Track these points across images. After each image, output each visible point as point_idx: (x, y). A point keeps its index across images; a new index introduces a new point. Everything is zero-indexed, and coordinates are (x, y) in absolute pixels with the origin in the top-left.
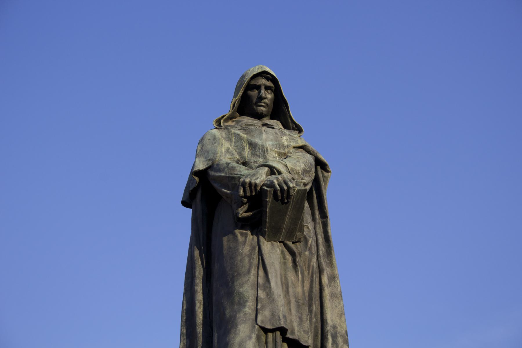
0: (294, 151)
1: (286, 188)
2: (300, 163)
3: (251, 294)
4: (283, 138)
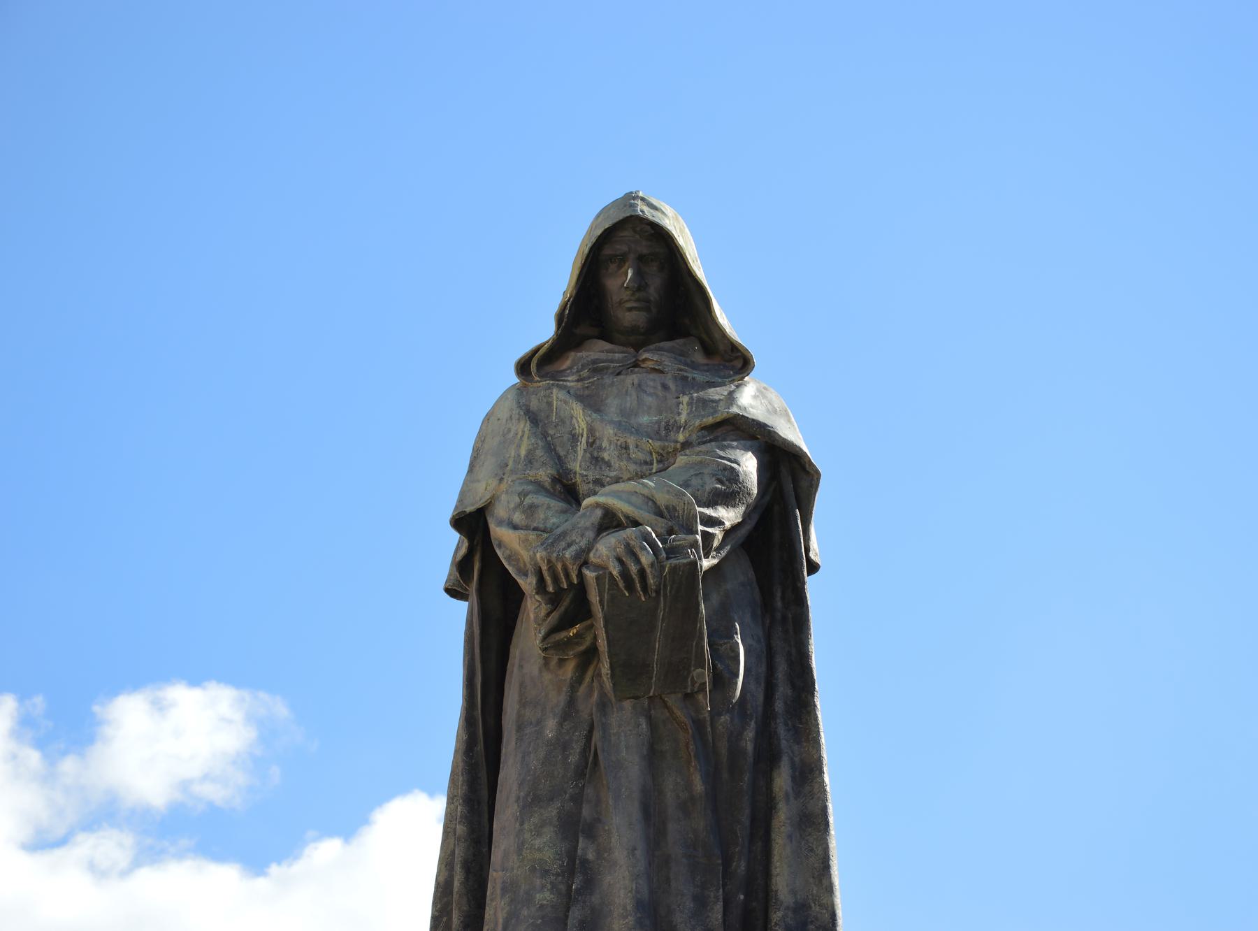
0: (704, 437)
1: (633, 568)
2: (702, 479)
3: (561, 851)
4: (681, 399)
